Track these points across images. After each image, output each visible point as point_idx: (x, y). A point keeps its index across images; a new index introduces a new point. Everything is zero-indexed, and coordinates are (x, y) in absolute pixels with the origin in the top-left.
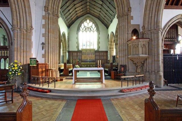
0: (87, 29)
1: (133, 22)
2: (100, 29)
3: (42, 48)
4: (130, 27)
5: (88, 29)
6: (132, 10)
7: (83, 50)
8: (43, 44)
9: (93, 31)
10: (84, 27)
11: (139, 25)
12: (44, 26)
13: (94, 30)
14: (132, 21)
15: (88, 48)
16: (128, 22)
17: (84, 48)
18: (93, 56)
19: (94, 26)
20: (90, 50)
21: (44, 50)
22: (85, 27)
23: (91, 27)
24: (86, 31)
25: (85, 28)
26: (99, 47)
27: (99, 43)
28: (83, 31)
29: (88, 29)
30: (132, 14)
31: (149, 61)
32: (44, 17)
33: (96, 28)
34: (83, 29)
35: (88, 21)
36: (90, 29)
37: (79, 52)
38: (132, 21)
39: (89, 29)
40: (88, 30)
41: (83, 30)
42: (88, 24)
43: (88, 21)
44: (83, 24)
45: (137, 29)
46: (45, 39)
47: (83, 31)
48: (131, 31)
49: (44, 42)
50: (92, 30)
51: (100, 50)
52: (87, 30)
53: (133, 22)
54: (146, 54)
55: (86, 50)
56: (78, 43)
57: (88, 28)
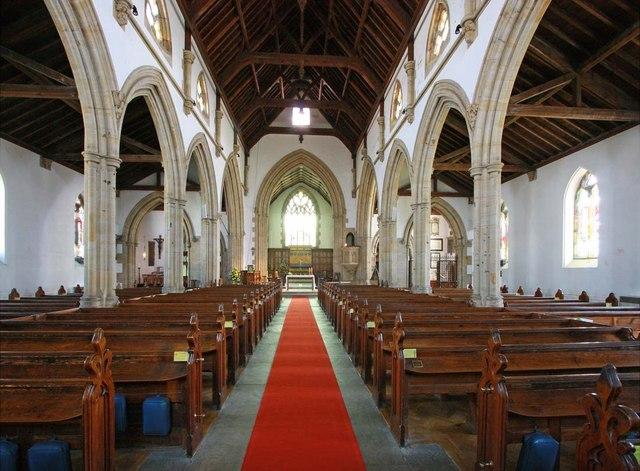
1: (348, 226)
2: (321, 212)
7: (291, 247)
15: (301, 243)
16: (344, 226)
17: (294, 243)
18: (309, 258)
19: (310, 203)
20: (304, 247)
23: (306, 205)
26: (318, 242)
27: (319, 234)
31: (360, 269)
35: (301, 194)
37: (286, 250)
43: (301, 194)
51: (320, 247)
53: (348, 226)
55: (297, 247)
56: (283, 234)
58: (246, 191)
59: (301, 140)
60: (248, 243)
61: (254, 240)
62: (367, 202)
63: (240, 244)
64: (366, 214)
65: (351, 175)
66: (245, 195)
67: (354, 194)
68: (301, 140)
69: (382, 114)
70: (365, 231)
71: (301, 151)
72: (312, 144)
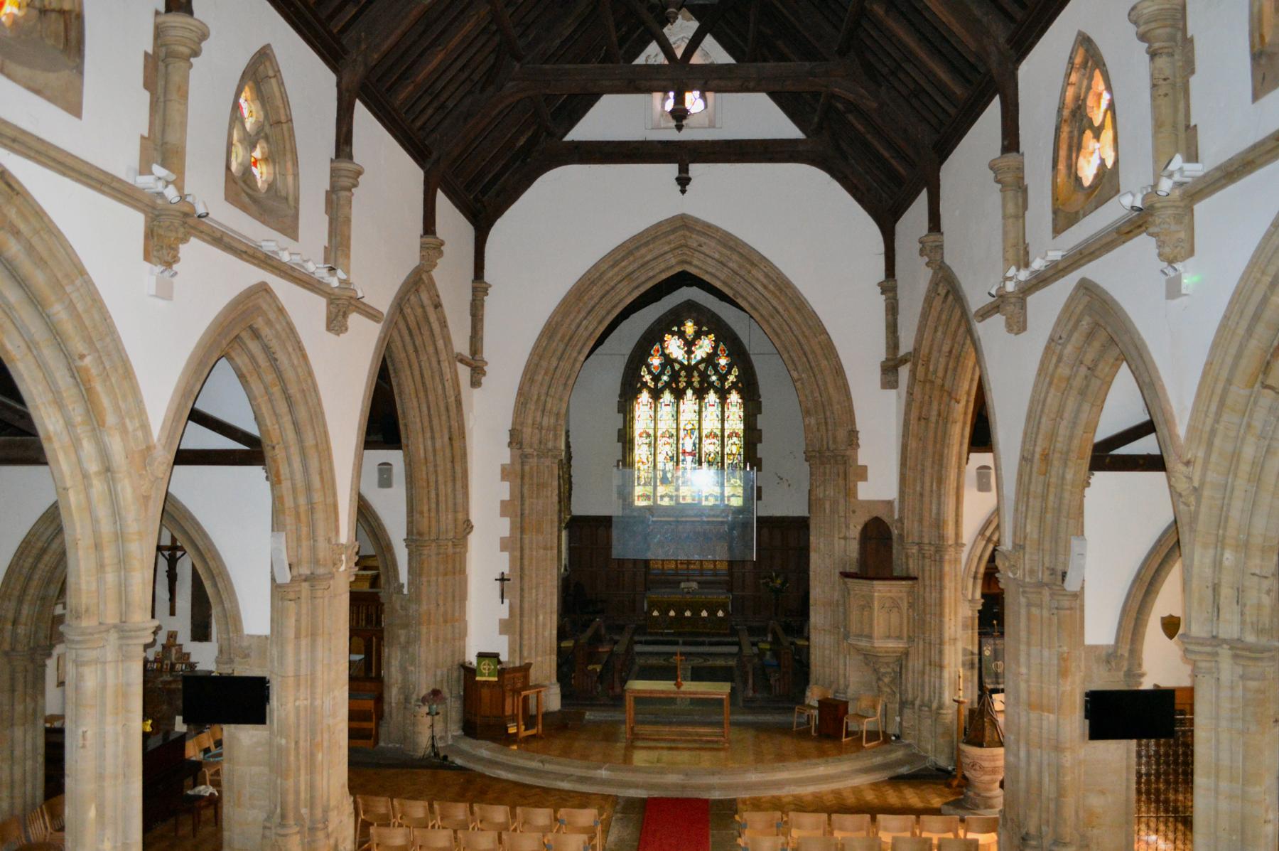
0: (683, 373)
3: (498, 593)
4: (854, 512)
5: (689, 376)
6: (863, 438)
8: (502, 579)
9: (723, 395)
10: (663, 366)
11: (890, 503)
12: (505, 508)
13: (727, 385)
14: (861, 485)
16: (850, 492)
21: (506, 601)
22: (668, 361)
23: (710, 360)
24: (679, 395)
25: (668, 370)
28: (656, 395)
29: (689, 376)
30: (863, 457)
31: (915, 663)
32: (506, 473)
33: (735, 371)
34: (656, 378)
36: (704, 377)
38: (861, 485)
39: (696, 380)
40: (689, 384)
41: (660, 385)
42: (689, 345)
44: (657, 346)
45: (886, 519)
46: (512, 560)
47: (656, 395)
48: (859, 528)
49: (507, 571)
50: (711, 385)
52: (682, 385)
53: (865, 491)
54: (899, 638)
57: (689, 369)
58: (478, 371)
59: (683, 181)
60: (485, 558)
61: (505, 545)
62: (945, 419)
63: (455, 568)
64: (942, 439)
65: (879, 302)
66: (475, 383)
67: (890, 370)
68: (683, 181)
69: (1011, 140)
70: (939, 524)
71: (683, 224)
72: (720, 195)
